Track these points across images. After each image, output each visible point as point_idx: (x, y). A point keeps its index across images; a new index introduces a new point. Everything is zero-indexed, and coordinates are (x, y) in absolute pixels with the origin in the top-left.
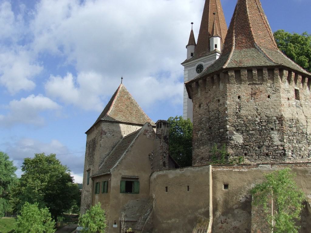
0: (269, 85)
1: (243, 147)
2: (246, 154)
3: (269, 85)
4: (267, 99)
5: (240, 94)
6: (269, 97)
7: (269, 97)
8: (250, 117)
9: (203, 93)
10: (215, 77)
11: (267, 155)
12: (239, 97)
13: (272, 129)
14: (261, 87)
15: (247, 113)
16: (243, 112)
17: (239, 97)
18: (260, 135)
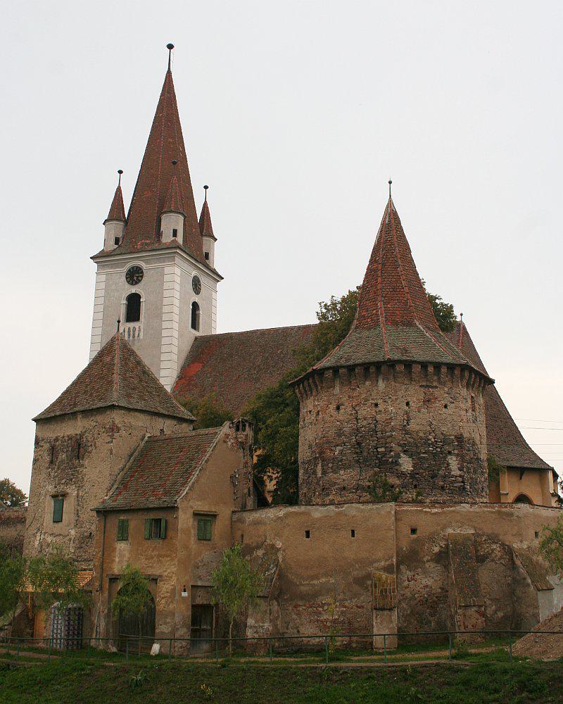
0: (446, 389)
1: (413, 475)
2: (415, 486)
3: (446, 389)
4: (444, 410)
5: (409, 400)
6: (446, 406)
7: (446, 406)
8: (421, 434)
9: (346, 388)
10: (372, 369)
11: (442, 488)
12: (408, 404)
13: (450, 453)
14: (437, 392)
15: (417, 428)
16: (413, 426)
17: (408, 404)
18: (435, 461)
